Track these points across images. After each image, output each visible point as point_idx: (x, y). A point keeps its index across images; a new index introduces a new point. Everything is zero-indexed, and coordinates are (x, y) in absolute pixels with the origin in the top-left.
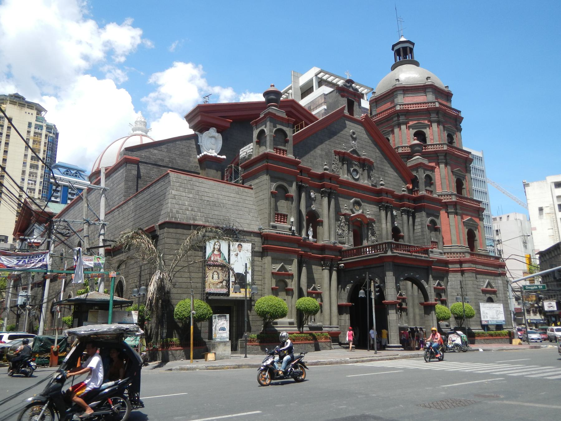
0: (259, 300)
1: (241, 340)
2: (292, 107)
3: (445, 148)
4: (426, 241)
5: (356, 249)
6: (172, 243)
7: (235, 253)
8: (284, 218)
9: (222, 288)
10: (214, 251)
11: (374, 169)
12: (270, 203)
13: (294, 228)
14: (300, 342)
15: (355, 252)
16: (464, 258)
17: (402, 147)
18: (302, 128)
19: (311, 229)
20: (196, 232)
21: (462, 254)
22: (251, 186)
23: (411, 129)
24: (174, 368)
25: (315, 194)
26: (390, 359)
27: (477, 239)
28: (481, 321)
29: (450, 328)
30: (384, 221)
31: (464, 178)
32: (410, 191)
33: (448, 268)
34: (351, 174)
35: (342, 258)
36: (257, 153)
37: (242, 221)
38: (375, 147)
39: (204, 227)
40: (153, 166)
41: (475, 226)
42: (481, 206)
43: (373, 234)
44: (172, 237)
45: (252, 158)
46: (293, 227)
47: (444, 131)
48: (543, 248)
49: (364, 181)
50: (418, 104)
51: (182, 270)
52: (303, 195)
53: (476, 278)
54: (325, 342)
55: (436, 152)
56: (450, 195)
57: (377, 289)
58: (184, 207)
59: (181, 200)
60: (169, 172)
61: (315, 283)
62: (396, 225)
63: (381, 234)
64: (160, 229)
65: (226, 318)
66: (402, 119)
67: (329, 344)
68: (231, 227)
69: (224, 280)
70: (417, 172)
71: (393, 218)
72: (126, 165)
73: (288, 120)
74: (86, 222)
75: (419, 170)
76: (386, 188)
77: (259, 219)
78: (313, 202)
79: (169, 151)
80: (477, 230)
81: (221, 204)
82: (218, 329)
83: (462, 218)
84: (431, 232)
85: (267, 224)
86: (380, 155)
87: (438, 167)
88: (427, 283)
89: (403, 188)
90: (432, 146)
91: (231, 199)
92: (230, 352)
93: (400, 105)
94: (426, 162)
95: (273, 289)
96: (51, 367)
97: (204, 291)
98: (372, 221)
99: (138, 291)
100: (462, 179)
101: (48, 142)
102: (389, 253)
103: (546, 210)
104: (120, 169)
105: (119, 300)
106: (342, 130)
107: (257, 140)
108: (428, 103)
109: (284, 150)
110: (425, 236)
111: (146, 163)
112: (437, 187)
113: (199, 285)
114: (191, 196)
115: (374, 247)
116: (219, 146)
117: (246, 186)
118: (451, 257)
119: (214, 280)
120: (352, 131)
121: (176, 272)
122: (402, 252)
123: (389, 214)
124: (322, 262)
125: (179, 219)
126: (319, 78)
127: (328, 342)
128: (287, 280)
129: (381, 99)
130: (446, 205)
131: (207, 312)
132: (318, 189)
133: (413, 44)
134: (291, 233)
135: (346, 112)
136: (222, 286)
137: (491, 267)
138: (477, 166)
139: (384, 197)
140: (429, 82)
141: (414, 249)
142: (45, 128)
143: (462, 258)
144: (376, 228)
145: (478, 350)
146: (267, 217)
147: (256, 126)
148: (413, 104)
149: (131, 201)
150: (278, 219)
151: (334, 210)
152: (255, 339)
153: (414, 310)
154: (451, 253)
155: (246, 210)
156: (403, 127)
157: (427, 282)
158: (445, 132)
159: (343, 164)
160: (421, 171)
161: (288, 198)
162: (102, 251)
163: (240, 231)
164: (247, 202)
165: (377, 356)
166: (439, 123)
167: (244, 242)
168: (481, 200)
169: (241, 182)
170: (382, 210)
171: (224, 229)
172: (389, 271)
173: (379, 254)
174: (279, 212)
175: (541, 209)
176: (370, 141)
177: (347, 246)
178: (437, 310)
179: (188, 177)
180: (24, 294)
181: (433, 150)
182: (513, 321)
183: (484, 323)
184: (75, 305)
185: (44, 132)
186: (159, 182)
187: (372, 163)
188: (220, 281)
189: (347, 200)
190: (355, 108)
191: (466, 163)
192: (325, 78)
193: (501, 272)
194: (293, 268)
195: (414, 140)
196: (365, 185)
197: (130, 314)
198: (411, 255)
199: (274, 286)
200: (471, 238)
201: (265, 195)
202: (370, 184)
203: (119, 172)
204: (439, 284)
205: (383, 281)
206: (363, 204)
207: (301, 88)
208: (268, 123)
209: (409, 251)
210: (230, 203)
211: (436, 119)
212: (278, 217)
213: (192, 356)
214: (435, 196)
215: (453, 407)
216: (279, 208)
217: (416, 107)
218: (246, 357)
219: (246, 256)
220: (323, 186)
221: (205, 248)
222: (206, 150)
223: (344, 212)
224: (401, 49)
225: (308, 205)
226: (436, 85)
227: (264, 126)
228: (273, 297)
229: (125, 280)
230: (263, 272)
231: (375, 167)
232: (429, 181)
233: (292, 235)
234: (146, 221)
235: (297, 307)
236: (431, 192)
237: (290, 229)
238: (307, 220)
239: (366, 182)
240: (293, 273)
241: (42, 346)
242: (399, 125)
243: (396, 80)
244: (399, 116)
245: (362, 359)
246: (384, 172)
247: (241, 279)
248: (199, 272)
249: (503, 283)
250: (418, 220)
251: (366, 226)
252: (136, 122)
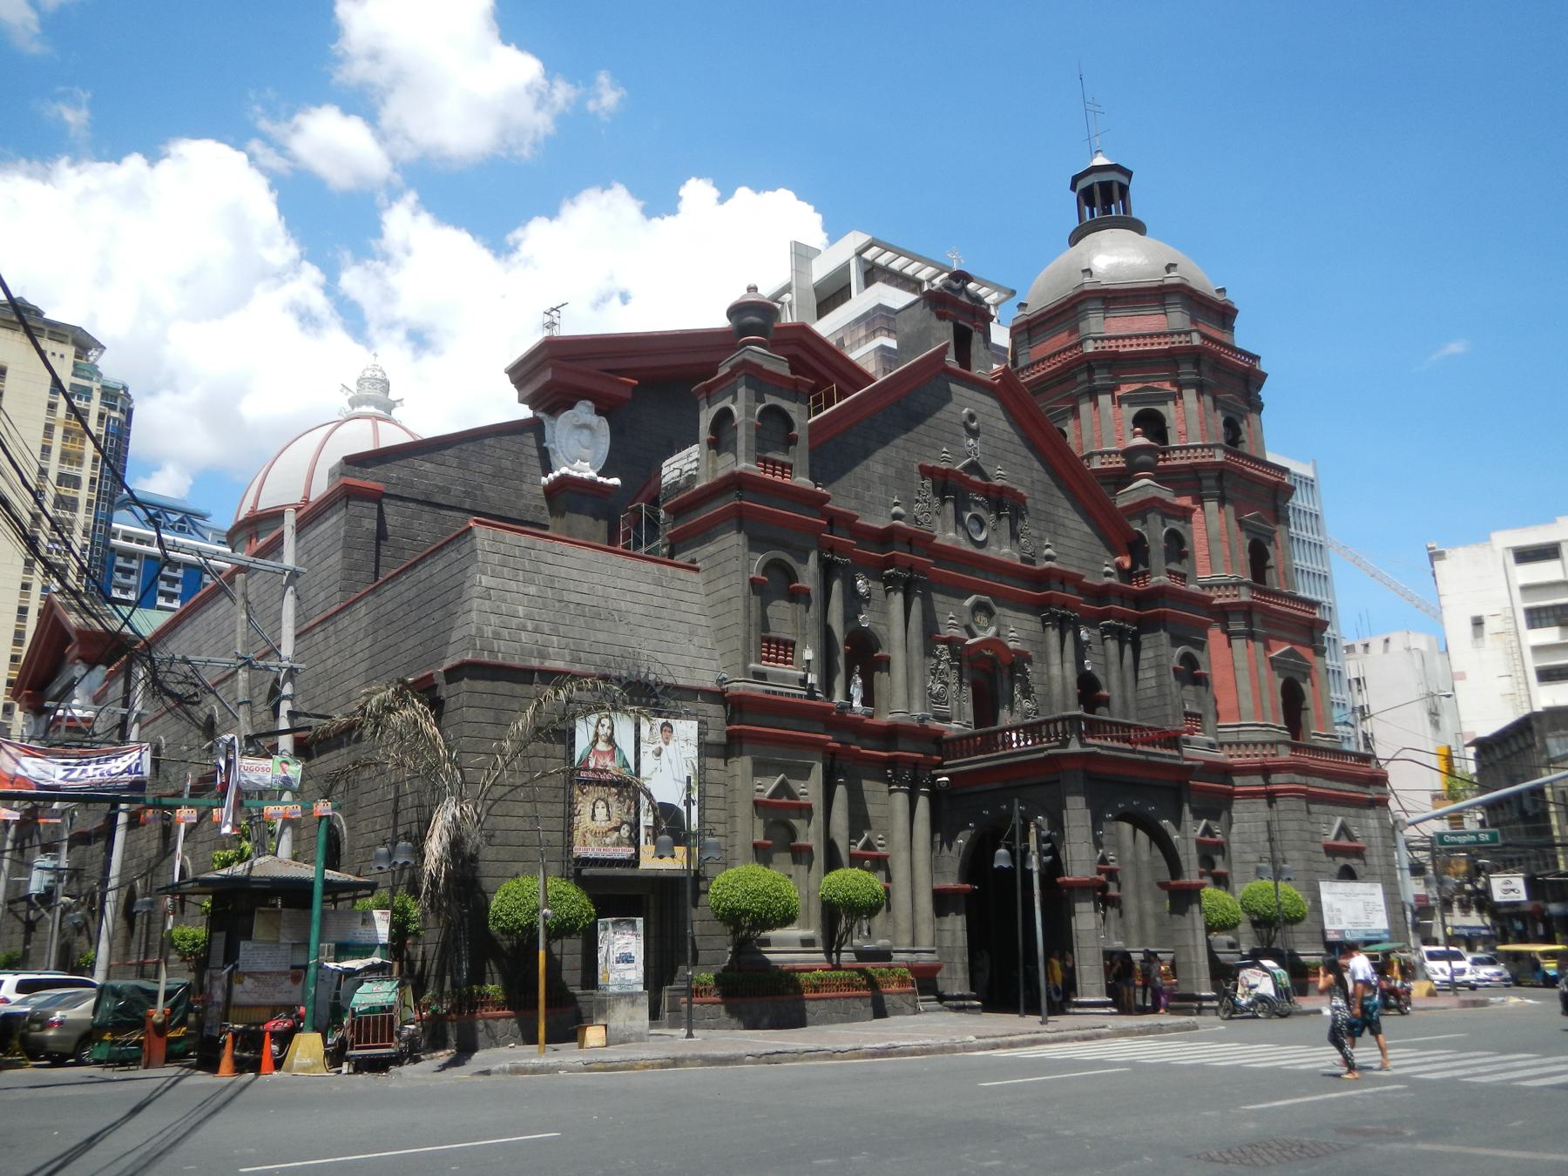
0: (721, 878)
1: (670, 990)
2: (801, 344)
3: (1219, 456)
4: (1169, 710)
5: (981, 735)
6: (482, 720)
7: (654, 747)
8: (786, 651)
9: (618, 845)
10: (596, 742)
11: (1027, 513)
12: (748, 609)
13: (812, 679)
14: (832, 994)
15: (978, 743)
16: (1274, 759)
17: (1102, 454)
18: (830, 403)
19: (859, 681)
20: (549, 691)
21: (1268, 746)
22: (694, 561)
23: (1125, 406)
24: (495, 1067)
25: (868, 583)
26: (1086, 1039)
27: (1308, 706)
28: (1323, 932)
29: (1240, 953)
30: (1055, 659)
31: (1271, 537)
32: (1125, 574)
33: (1230, 787)
34: (965, 528)
35: (944, 760)
36: (710, 473)
37: (671, 658)
38: (1031, 455)
39: (575, 677)
40: (420, 507)
41: (1304, 670)
42: (1318, 616)
43: (1027, 693)
44: (481, 705)
45: (697, 486)
46: (809, 675)
47: (1215, 410)
48: (1486, 730)
49: (1001, 549)
50: (1144, 336)
51: (509, 797)
52: (837, 586)
53: (1309, 812)
54: (900, 993)
55: (1194, 469)
56: (1235, 585)
57: (1046, 846)
58: (514, 622)
59: (505, 601)
60: (471, 524)
61: (868, 827)
62: (1089, 669)
63: (1048, 695)
64: (449, 682)
65: (634, 929)
66: (1101, 378)
67: (910, 999)
68: (643, 675)
69: (623, 823)
70: (1145, 522)
71: (1081, 649)
72: (347, 504)
73: (796, 384)
74: (244, 665)
75: (1150, 516)
76: (1061, 568)
77: (717, 654)
78: (864, 606)
79: (463, 465)
80: (1308, 680)
81: (613, 612)
82: (612, 958)
83: (1268, 648)
84: (1183, 686)
85: (740, 666)
86: (1047, 478)
87: (1199, 510)
88: (1178, 827)
89: (1107, 565)
90: (1184, 452)
91: (642, 598)
92: (647, 1022)
93: (1095, 340)
94: (1166, 494)
95: (756, 846)
96: (146, 1068)
97: (570, 852)
98: (1024, 657)
99: (390, 856)
100: (1264, 539)
101: (107, 434)
102: (1074, 747)
103: (1490, 625)
104: (329, 512)
105: (339, 879)
106: (939, 408)
107: (709, 436)
108: (1172, 334)
109: (784, 465)
110: (1169, 698)
111: (401, 498)
112: (1199, 564)
113: (557, 837)
114: (532, 590)
115: (1030, 730)
116: (602, 452)
117: (681, 562)
118: (1240, 756)
119: (598, 823)
120: (966, 409)
121: (495, 801)
122: (1108, 743)
123: (1069, 636)
124: (888, 772)
125: (500, 655)
126: (866, 261)
127: (909, 993)
128: (795, 822)
129: (1042, 323)
130: (1223, 614)
131: (581, 912)
132: (875, 571)
133: (1129, 174)
134: (805, 693)
135: (951, 360)
136: (618, 838)
137: (1349, 782)
138: (1300, 502)
139: (1055, 591)
140: (1173, 278)
141: (1142, 736)
142: (97, 395)
143: (1269, 758)
144: (1035, 676)
145: (1319, 1012)
146: (740, 647)
147: (708, 397)
148: (1130, 337)
149: (362, 603)
150: (769, 653)
151: (920, 627)
152: (708, 987)
153: (1140, 901)
154: (1238, 744)
155: (685, 628)
156: (1104, 400)
157: (1178, 823)
158: (1219, 412)
159: (943, 502)
160: (1154, 519)
161: (798, 596)
162: (285, 742)
163: (667, 686)
164: (683, 606)
165: (1049, 1030)
166: (1201, 389)
167: (678, 716)
168: (1319, 598)
169: (665, 550)
170: (1050, 629)
171: (624, 682)
172: (1077, 793)
173: (1046, 749)
174: (772, 634)
175: (1478, 623)
176: (1016, 439)
177: (957, 726)
178: (1206, 903)
179: (525, 540)
180: (48, 863)
181: (1184, 462)
182: (1410, 932)
183: (1331, 937)
184: (214, 894)
185: (95, 406)
186: (444, 552)
187: (1021, 499)
189: (955, 601)
190: (974, 349)
191: (1275, 498)
192: (882, 261)
193: (1376, 796)
194: (810, 789)
195: (1135, 435)
196: (1005, 559)
197: (367, 920)
198: (1133, 751)
199: (759, 838)
200: (1293, 703)
201: (734, 587)
202: (1017, 556)
203: (322, 527)
204: (1207, 831)
205: (1057, 824)
206: (997, 610)
207: (818, 289)
208: (742, 391)
209: (1127, 740)
210: (638, 609)
211: (1193, 377)
212: (769, 648)
213: (542, 1035)
214: (1193, 587)
215: (1285, 1160)
216: (773, 624)
217: (1138, 345)
218: (690, 1035)
219: (683, 756)
220: (890, 562)
221: (573, 735)
222: (565, 460)
223: (947, 632)
224: (1097, 188)
225: (850, 616)
226: (1192, 285)
227: (731, 398)
228: (759, 869)
229: (347, 825)
230: (729, 800)
231: (1029, 509)
232: (1177, 547)
233: (808, 697)
234: (406, 660)
235: (823, 895)
236: (1183, 577)
237: (803, 681)
238: (848, 655)
239: (1006, 550)
240: (810, 802)
241: (120, 1010)
242: (1092, 395)
243: (1084, 271)
244: (1093, 370)
245: (1010, 1038)
246: (1054, 522)
247: (669, 821)
248: (556, 800)
249: (1382, 827)
250: (1147, 654)
251: (1006, 671)
252: (360, 382)
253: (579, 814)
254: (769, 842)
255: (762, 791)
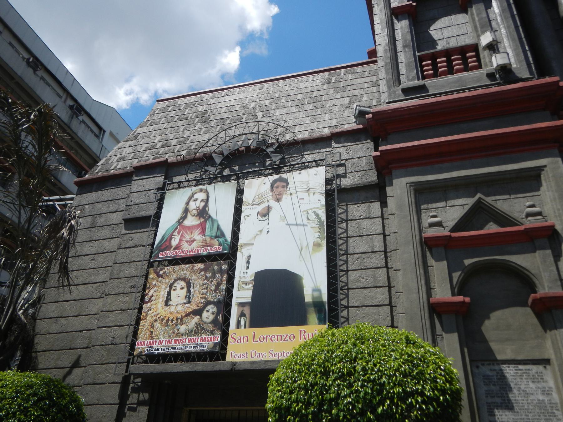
7: (260, 208)
9: (197, 333)
10: (184, 218)
69: (207, 303)
119: (173, 309)
171: (226, 153)
188: (193, 307)
219: (303, 208)
240: (548, 224)
253: (149, 301)
254: (460, 299)
255: (439, 224)
